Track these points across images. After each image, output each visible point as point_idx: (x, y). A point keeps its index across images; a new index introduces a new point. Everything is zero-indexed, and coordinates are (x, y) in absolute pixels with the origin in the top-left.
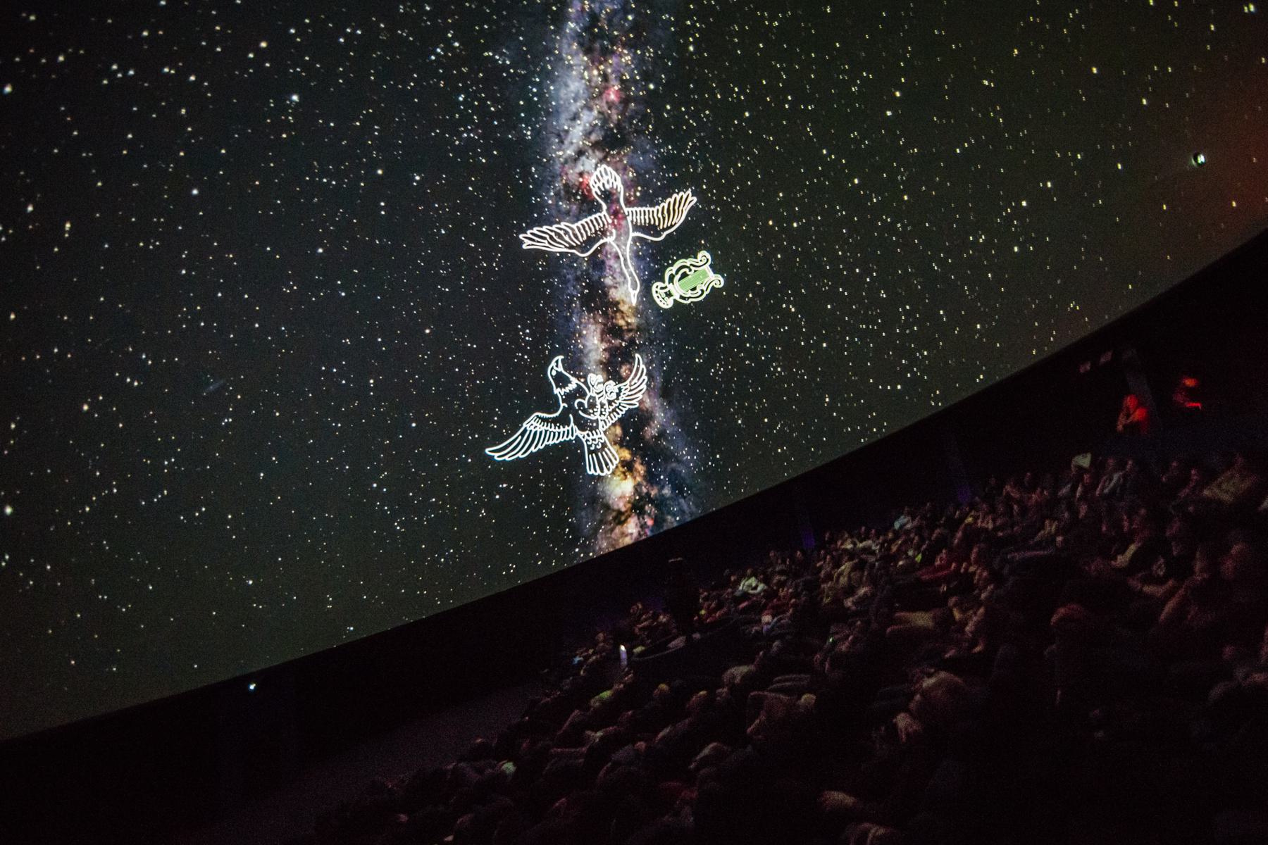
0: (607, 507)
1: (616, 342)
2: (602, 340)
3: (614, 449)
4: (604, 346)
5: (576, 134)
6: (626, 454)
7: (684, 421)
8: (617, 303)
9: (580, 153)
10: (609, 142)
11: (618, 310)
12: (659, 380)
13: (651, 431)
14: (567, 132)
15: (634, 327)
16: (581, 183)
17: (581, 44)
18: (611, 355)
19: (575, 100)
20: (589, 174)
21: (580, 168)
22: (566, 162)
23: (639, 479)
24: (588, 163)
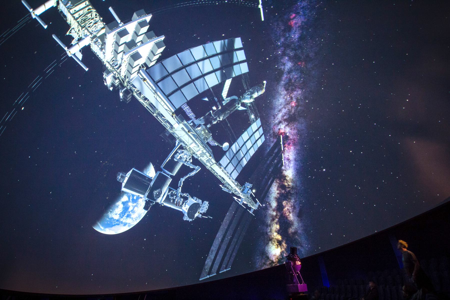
0: (268, 258)
1: (283, 191)
2: (278, 190)
3: (275, 234)
4: (278, 192)
5: (280, 116)
6: (279, 237)
7: (306, 230)
8: (286, 176)
9: (280, 122)
10: (290, 119)
11: (285, 179)
12: (297, 210)
13: (291, 230)
14: (277, 115)
15: (291, 186)
17: (284, 88)
18: (280, 196)
19: (281, 105)
21: (279, 127)
22: (275, 125)
23: (283, 249)
24: (282, 126)
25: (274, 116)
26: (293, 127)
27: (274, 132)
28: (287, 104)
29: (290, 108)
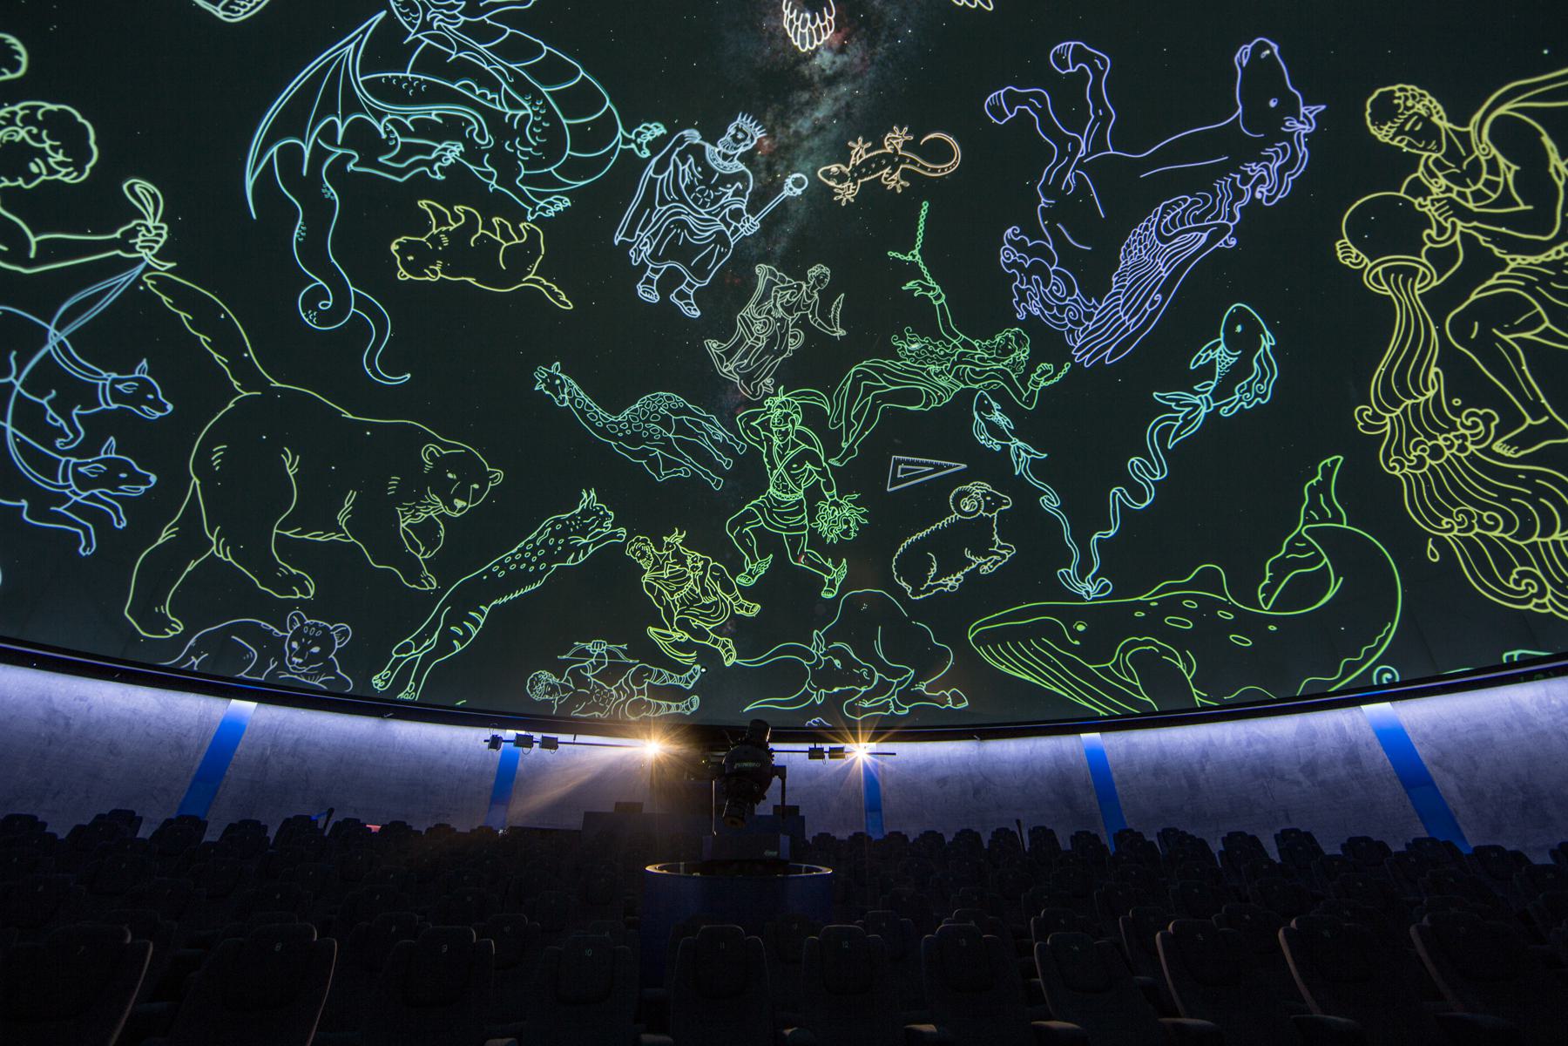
14: (836, 115)
16: (847, 37)
20: (828, 46)
21: (840, 60)
22: (855, 77)
24: (825, 60)
25: (849, 116)
26: (779, 45)
27: (872, 44)
28: (787, 148)
29: (778, 130)
